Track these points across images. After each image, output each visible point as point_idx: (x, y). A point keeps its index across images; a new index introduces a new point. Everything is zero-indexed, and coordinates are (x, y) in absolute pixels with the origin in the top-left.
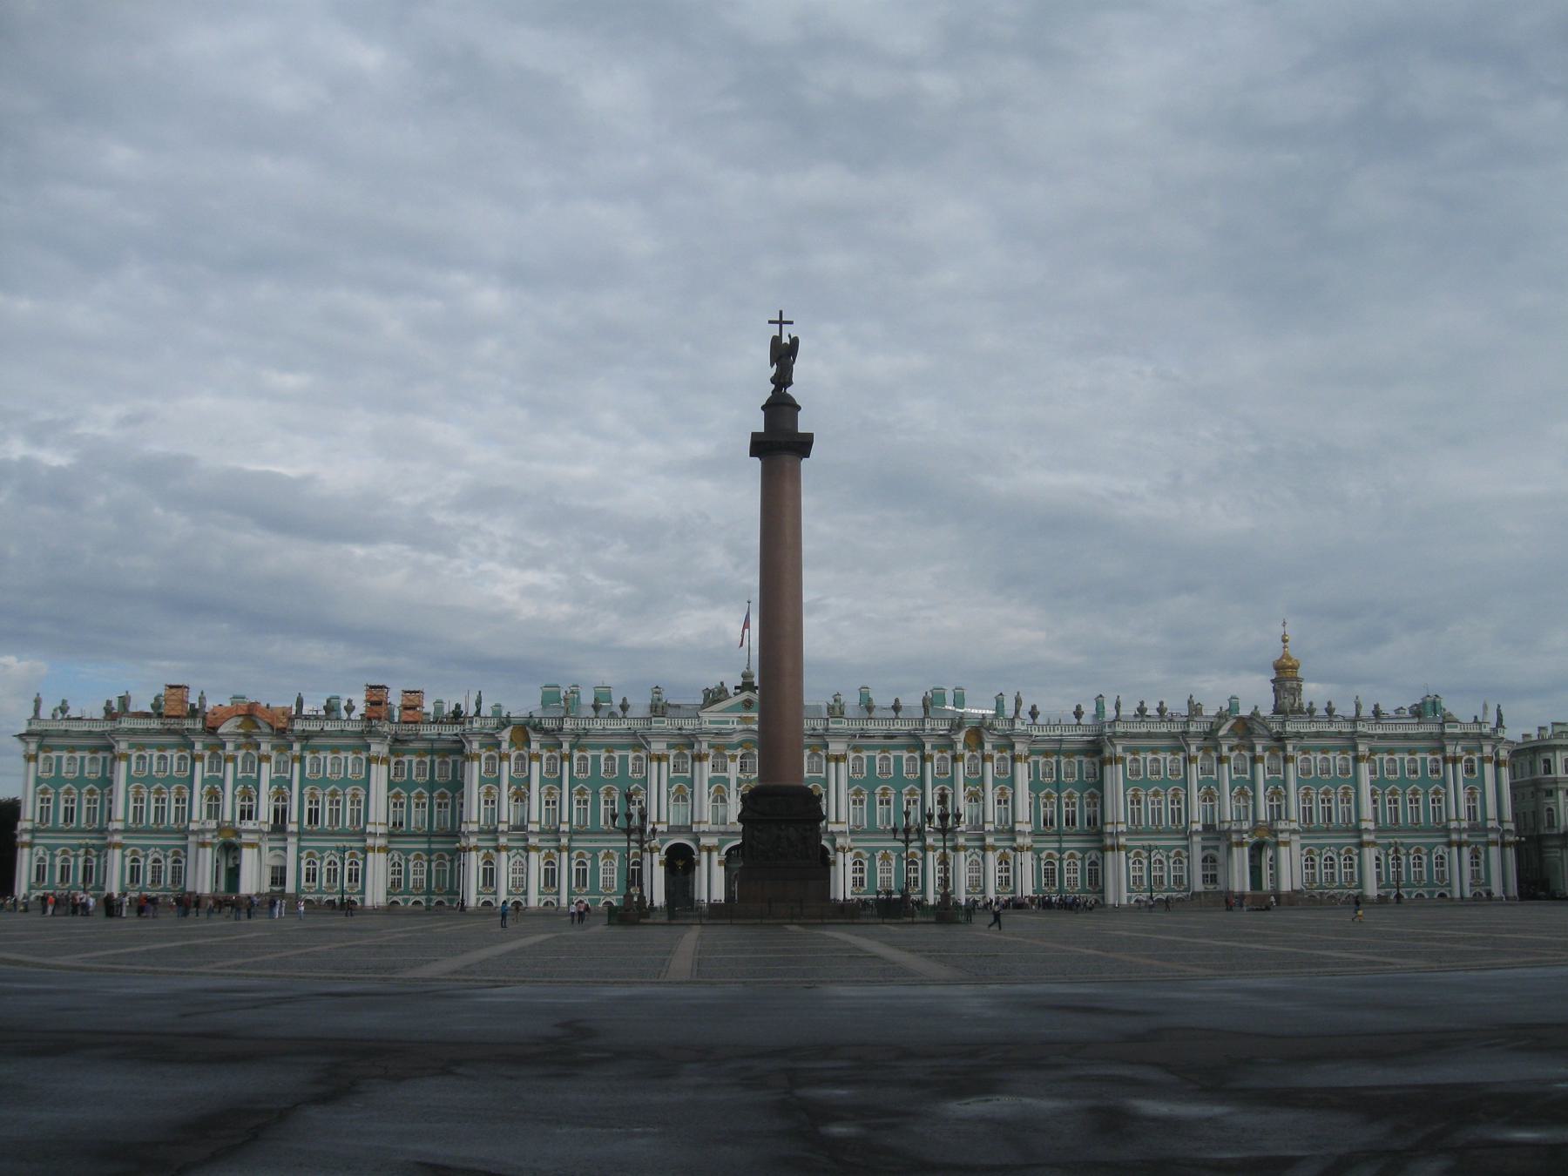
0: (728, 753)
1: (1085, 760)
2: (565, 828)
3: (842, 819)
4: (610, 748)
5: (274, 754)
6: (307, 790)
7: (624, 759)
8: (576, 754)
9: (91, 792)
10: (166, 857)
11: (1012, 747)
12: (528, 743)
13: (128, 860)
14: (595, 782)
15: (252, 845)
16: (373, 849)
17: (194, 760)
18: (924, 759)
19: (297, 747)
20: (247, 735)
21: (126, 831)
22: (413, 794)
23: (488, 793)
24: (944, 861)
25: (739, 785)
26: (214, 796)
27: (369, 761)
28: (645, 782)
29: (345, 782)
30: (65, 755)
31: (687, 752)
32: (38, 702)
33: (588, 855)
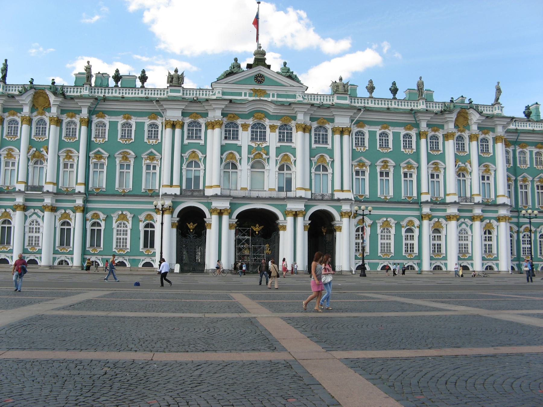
0: (240, 122)
1: (535, 150)
2: (81, 189)
3: (346, 187)
4: (128, 115)
7: (140, 126)
8: (95, 120)
11: (493, 130)
12: (48, 107)
14: (111, 146)
18: (419, 135)
24: (437, 230)
25: (250, 153)
28: (159, 147)
31: (202, 121)
33: (102, 216)
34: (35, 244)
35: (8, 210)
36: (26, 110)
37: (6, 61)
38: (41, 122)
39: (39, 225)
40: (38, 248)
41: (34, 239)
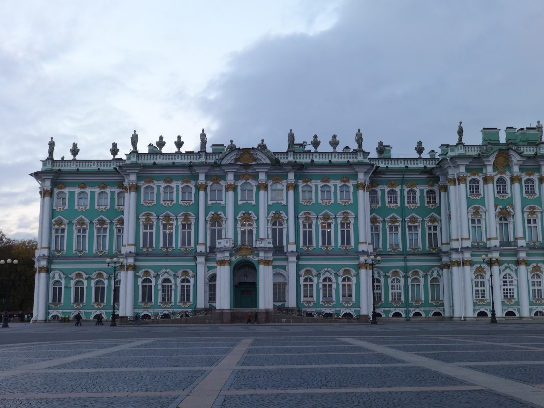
5: (270, 183)
6: (301, 215)
9: (102, 222)
10: (175, 276)
13: (140, 281)
15: (267, 263)
16: (365, 265)
17: (198, 188)
19: (291, 176)
20: (247, 166)
21: (137, 255)
22: (388, 219)
23: (477, 212)
26: (216, 221)
27: (357, 187)
29: (335, 206)
30: (77, 190)
32: (52, 145)
34: (510, 296)
35: (482, 265)
36: (490, 169)
37: (461, 123)
38: (501, 180)
39: (512, 278)
40: (514, 301)
41: (509, 291)
